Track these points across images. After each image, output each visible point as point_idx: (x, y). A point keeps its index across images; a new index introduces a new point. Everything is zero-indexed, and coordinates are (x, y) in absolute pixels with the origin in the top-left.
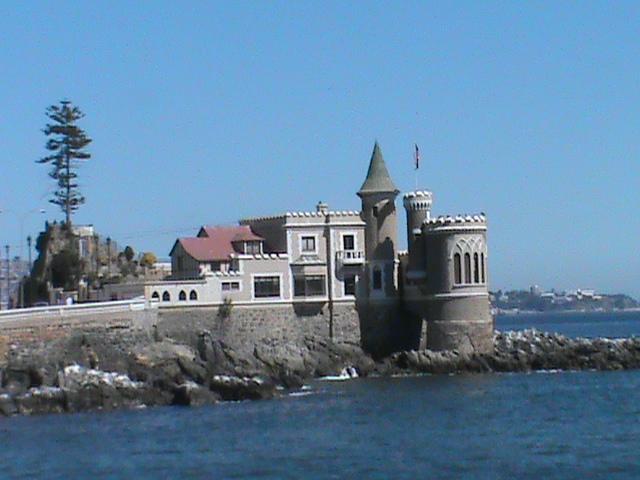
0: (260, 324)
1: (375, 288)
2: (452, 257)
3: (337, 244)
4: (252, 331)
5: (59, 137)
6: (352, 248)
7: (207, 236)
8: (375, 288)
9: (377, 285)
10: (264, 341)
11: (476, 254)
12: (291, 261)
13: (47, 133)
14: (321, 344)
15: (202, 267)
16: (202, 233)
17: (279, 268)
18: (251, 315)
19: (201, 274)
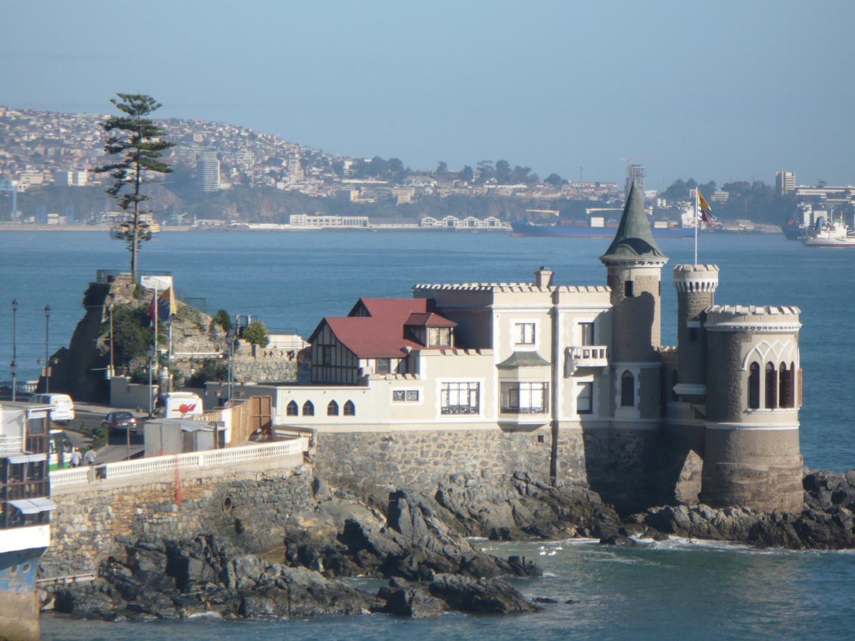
0: (449, 454)
1: (624, 403)
2: (746, 368)
4: (436, 463)
5: (127, 135)
7: (368, 314)
8: (624, 403)
9: (627, 401)
12: (498, 360)
13: (108, 128)
14: (538, 486)
16: (359, 309)
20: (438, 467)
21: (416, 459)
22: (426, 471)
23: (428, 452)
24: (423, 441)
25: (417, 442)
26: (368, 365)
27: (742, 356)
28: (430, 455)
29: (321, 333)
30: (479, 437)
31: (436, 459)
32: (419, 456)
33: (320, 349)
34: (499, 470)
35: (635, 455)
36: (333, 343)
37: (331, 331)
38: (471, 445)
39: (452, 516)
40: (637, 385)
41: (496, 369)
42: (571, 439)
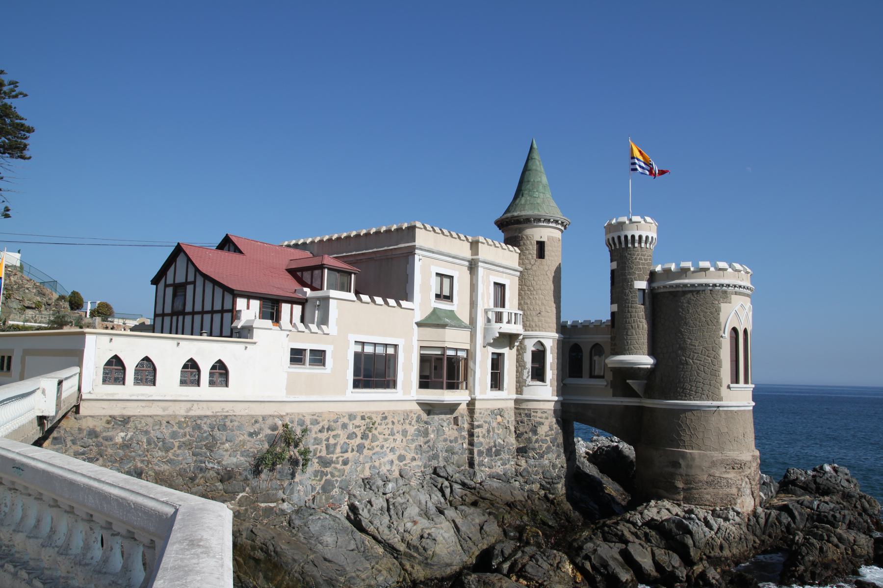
0: (361, 448)
3: (486, 298)
6: (503, 306)
10: (367, 483)
11: (735, 330)
12: (418, 319)
15: (241, 303)
16: (227, 244)
17: (398, 328)
18: (344, 426)
19: (239, 324)
20: (348, 467)
21: (320, 457)
22: (333, 475)
23: (335, 445)
24: (328, 429)
25: (320, 431)
26: (248, 308)
27: (722, 319)
28: (338, 450)
29: (173, 266)
30: (396, 421)
31: (346, 455)
32: (324, 454)
33: (170, 291)
34: (416, 466)
35: (548, 438)
36: (191, 278)
37: (189, 260)
38: (387, 432)
39: (380, 550)
40: (551, 359)
41: (415, 326)
42: (485, 422)
